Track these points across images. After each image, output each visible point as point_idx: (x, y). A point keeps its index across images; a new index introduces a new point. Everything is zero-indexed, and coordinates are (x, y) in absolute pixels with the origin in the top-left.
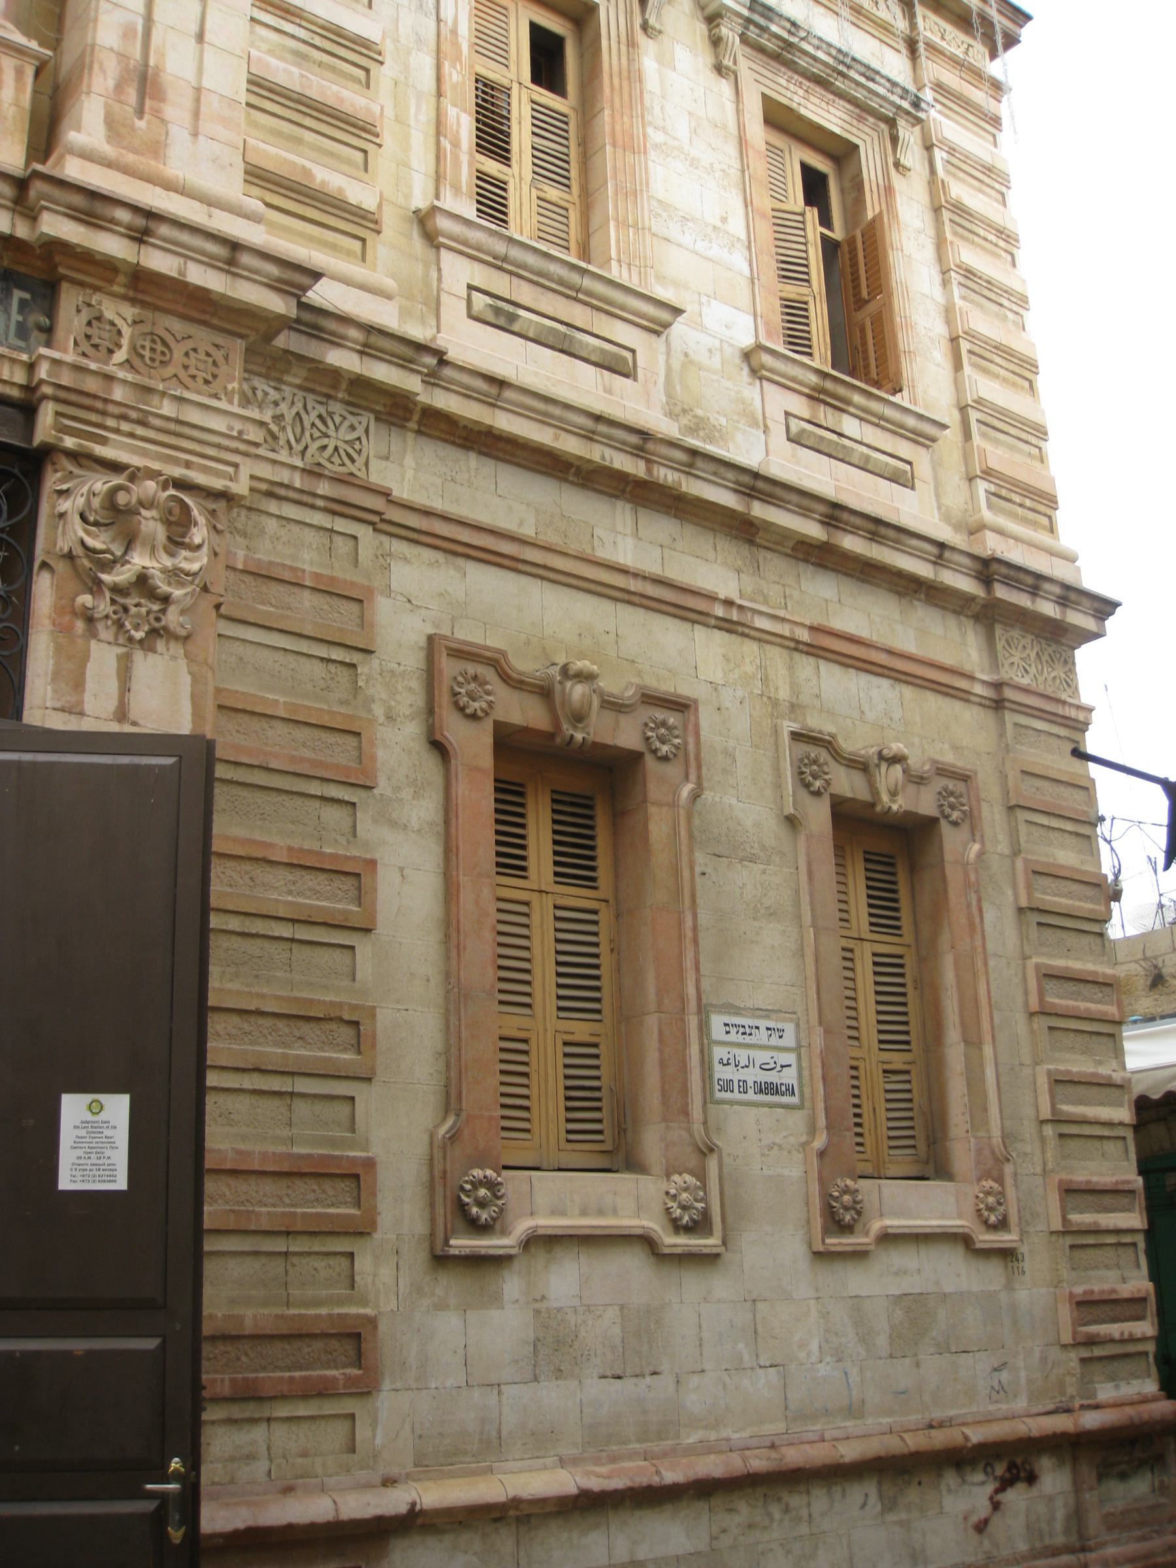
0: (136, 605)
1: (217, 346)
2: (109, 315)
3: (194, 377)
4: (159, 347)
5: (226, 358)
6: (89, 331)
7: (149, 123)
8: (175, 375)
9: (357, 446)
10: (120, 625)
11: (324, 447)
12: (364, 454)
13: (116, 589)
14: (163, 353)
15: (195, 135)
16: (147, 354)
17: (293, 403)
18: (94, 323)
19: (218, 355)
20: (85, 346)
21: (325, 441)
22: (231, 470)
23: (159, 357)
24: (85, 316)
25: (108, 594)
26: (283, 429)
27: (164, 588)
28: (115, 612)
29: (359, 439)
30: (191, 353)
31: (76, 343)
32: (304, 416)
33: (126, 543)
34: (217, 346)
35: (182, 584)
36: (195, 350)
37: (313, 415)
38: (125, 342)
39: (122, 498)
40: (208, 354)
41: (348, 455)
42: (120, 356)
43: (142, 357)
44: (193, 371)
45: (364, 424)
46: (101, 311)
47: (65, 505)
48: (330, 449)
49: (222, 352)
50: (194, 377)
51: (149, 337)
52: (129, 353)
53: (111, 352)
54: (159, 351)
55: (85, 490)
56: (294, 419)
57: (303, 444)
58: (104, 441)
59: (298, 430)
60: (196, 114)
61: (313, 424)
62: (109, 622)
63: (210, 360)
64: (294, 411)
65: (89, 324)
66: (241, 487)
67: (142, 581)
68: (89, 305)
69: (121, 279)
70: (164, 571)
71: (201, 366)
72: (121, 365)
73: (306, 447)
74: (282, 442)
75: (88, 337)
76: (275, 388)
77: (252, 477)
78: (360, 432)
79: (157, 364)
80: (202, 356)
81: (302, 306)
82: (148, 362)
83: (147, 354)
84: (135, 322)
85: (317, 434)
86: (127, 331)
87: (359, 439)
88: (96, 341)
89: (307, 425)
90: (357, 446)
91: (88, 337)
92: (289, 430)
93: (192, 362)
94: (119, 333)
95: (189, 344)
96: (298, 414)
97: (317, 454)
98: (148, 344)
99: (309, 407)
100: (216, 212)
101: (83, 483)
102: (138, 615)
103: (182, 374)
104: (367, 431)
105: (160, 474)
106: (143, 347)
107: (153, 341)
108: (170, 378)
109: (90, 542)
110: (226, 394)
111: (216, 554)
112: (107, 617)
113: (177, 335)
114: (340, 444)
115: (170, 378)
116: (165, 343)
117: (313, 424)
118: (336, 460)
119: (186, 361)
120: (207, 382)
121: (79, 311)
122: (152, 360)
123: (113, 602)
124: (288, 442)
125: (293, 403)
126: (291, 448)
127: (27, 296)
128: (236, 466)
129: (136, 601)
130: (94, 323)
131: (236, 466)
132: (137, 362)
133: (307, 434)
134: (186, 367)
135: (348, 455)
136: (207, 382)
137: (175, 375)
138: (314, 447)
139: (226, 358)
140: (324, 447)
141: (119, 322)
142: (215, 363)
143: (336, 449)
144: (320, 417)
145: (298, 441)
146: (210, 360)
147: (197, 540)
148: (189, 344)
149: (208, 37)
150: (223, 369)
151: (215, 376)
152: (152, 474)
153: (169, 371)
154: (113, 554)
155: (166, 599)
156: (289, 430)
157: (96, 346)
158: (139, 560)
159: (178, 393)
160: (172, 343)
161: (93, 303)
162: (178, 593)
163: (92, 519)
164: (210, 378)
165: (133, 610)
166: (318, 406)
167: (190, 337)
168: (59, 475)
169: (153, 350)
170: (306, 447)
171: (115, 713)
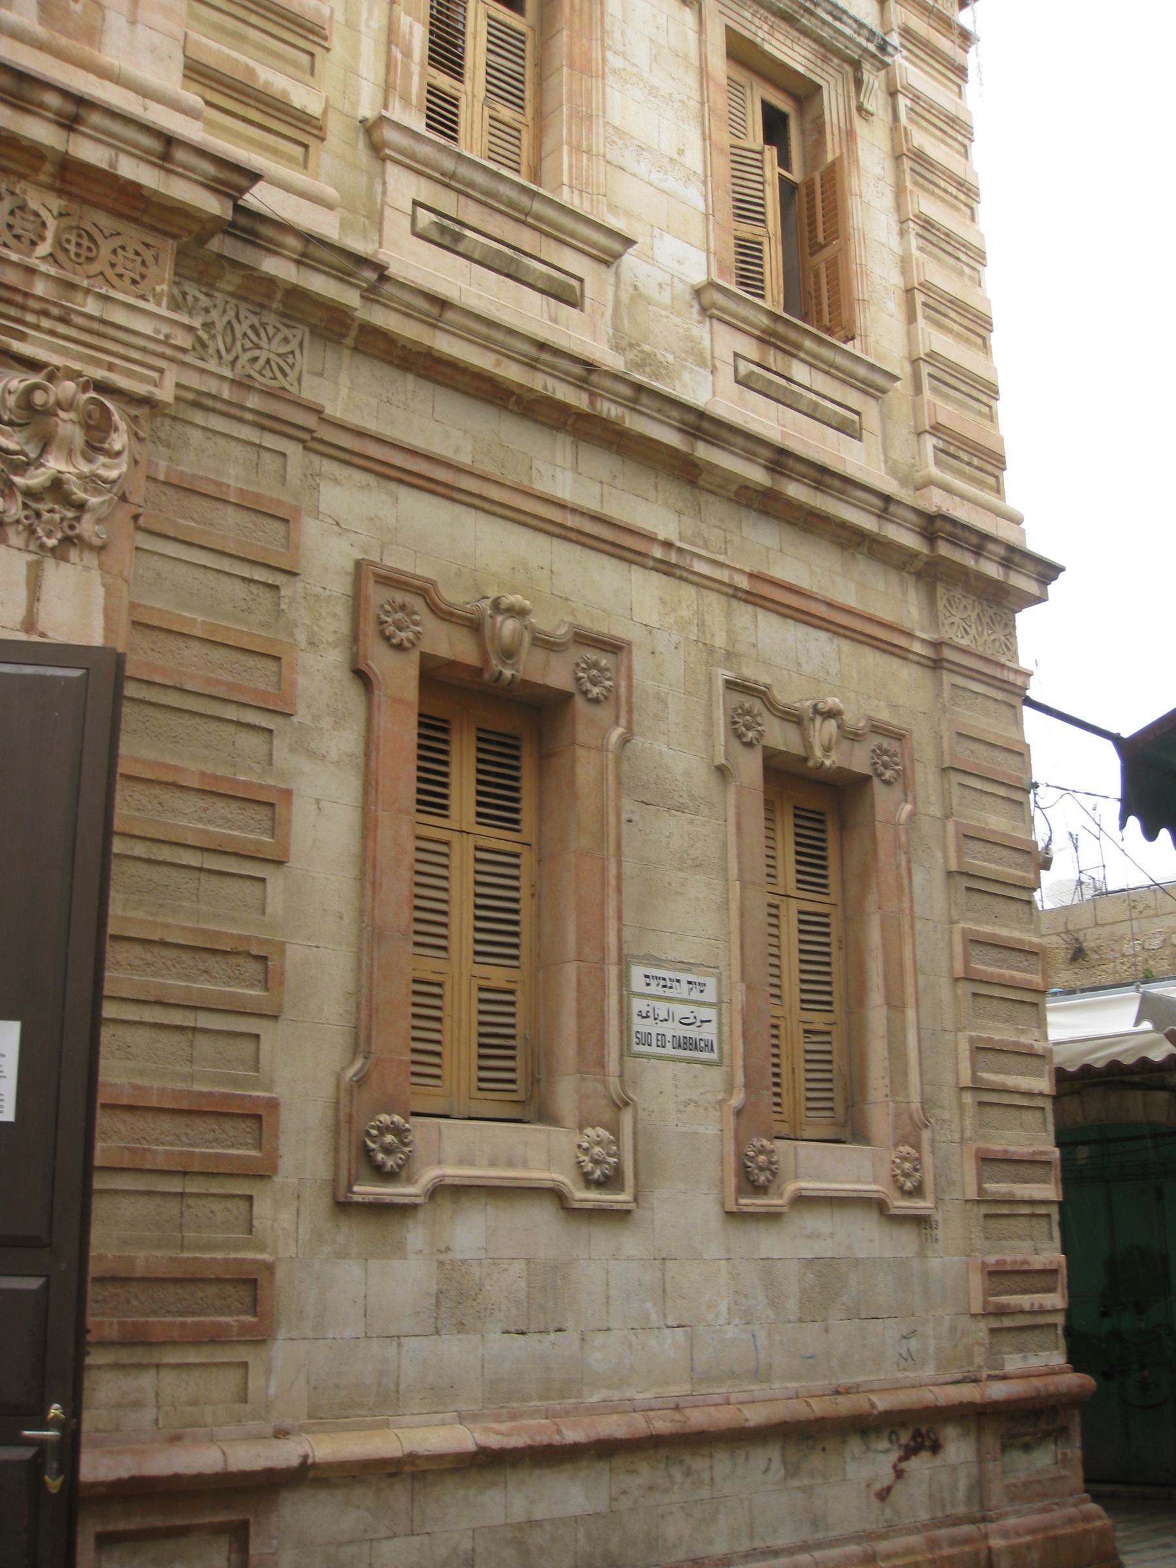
0: (51, 511)
1: (147, 245)
2: (33, 205)
3: (120, 276)
4: (85, 242)
5: (156, 258)
6: (12, 221)
8: (102, 273)
9: (290, 360)
10: (31, 531)
11: (255, 359)
12: (297, 368)
13: (30, 494)
14: (89, 249)
16: (72, 248)
17: (225, 311)
18: (18, 212)
19: (148, 255)
21: (257, 353)
22: (155, 375)
23: (84, 253)
25: (20, 498)
26: (214, 337)
27: (80, 494)
28: (27, 518)
29: (292, 352)
33: (41, 445)
34: (147, 245)
35: (98, 492)
36: (123, 248)
37: (245, 325)
38: (50, 234)
39: (39, 398)
40: (137, 253)
42: (44, 249)
43: (67, 251)
45: (299, 338)
46: (25, 201)
48: (262, 362)
49: (152, 252)
50: (120, 276)
51: (75, 231)
52: (53, 246)
53: (33, 243)
54: (85, 246)
56: (225, 328)
57: (234, 354)
58: (22, 337)
59: (229, 339)
62: (20, 528)
64: (225, 319)
65: (12, 213)
66: (165, 394)
67: (57, 485)
68: (13, 193)
69: (48, 167)
70: (81, 476)
71: (130, 265)
72: (43, 258)
73: (237, 358)
74: (211, 351)
76: (207, 295)
77: (178, 385)
78: (293, 345)
79: (82, 260)
80: (130, 255)
81: (239, 209)
82: (73, 257)
83: (72, 248)
84: (61, 215)
85: (248, 345)
86: (52, 224)
87: (292, 352)
88: (19, 231)
89: (239, 334)
90: (290, 360)
92: (220, 338)
93: (119, 260)
94: (44, 225)
95: (117, 242)
96: (229, 323)
97: (248, 366)
98: (73, 238)
99: (242, 317)
100: (152, 105)
102: (51, 522)
103: (110, 273)
104: (301, 345)
105: (80, 374)
106: (68, 241)
107: (80, 236)
108: (95, 276)
110: (154, 296)
111: (136, 462)
112: (18, 522)
113: (104, 230)
114: (273, 357)
115: (95, 276)
116: (92, 239)
117: (245, 335)
118: (267, 373)
119: (113, 259)
120: (134, 282)
122: (78, 255)
123: (25, 506)
124: (218, 351)
125: (225, 311)
126: (220, 357)
128: (161, 371)
129: (50, 506)
130: (18, 212)
131: (161, 371)
132: (61, 257)
133: (238, 344)
134: (113, 265)
136: (134, 282)
137: (102, 273)
139: (156, 258)
140: (255, 359)
142: (144, 263)
143: (268, 361)
144: (252, 327)
145: (228, 351)
146: (139, 259)
147: (117, 447)
150: (152, 269)
151: (143, 277)
152: (73, 375)
153: (95, 268)
154: (26, 455)
155: (81, 507)
156: (220, 338)
158: (55, 464)
159: (103, 291)
160: (100, 239)
161: (18, 191)
162: (93, 500)
164: (138, 278)
165: (46, 516)
166: (251, 316)
167: (118, 234)
169: (79, 245)
170: (237, 358)
171: (22, 623)
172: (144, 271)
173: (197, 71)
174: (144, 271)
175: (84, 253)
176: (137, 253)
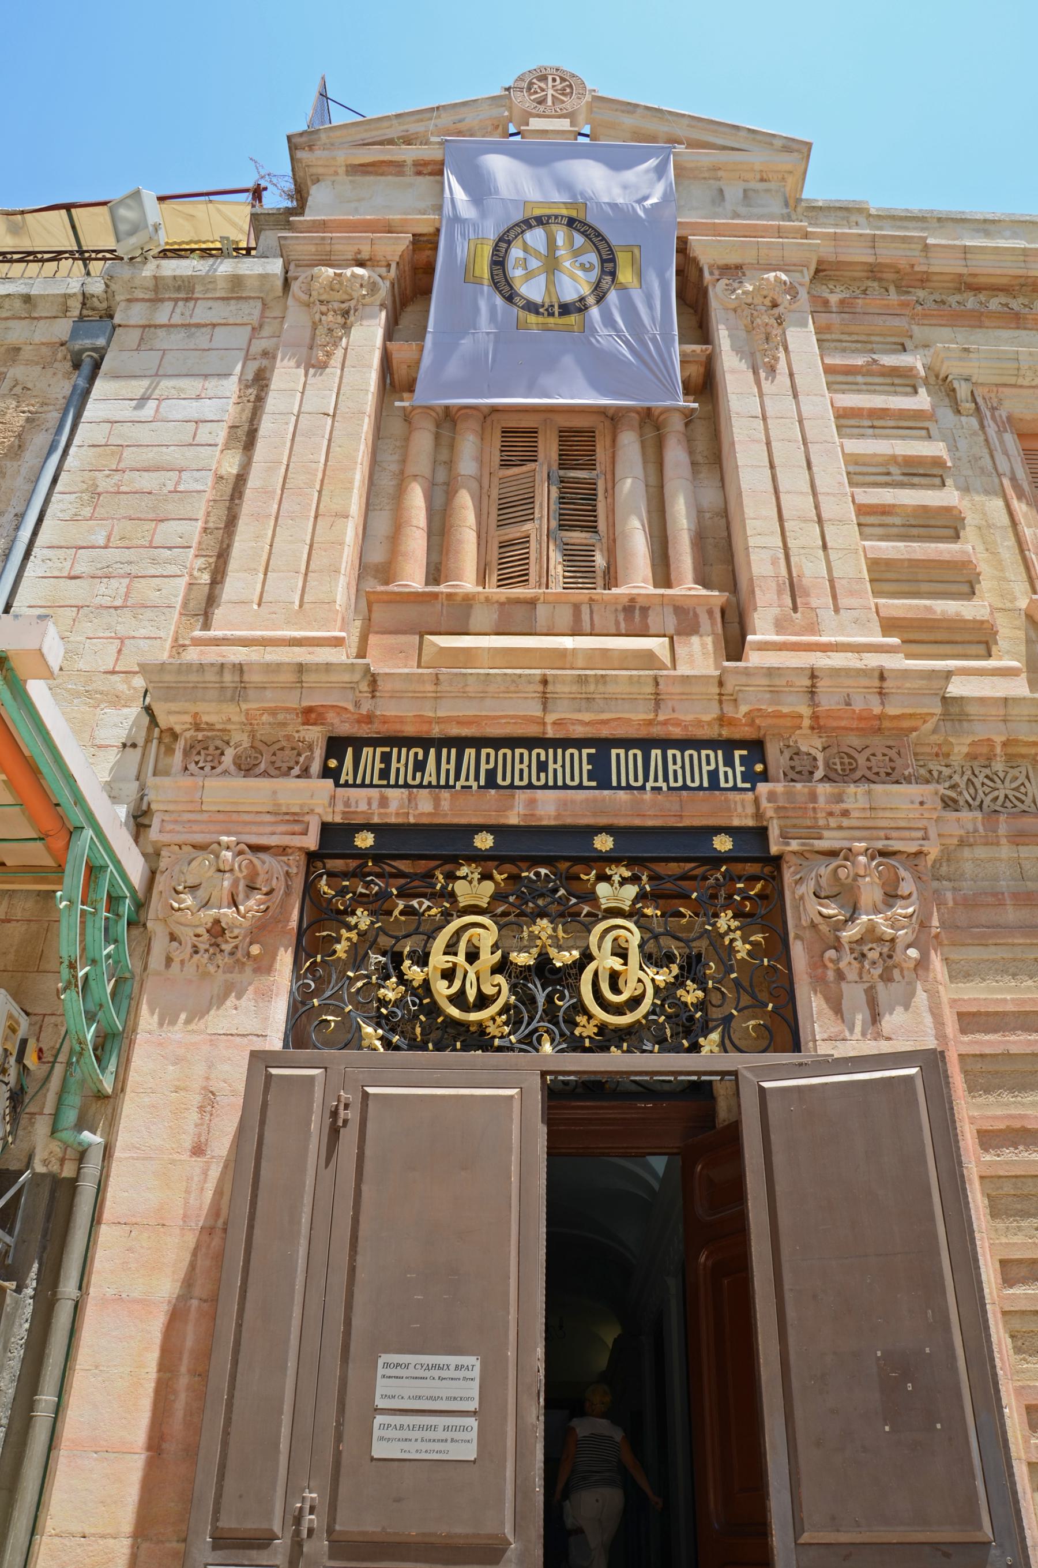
1: (890, 747)
2: (804, 749)
3: (877, 774)
4: (846, 760)
5: (899, 754)
6: (793, 763)
7: (803, 613)
8: (863, 776)
9: (1023, 790)
11: (997, 798)
12: (1030, 794)
15: (837, 610)
17: (963, 773)
18: (795, 757)
20: (792, 775)
21: (996, 793)
24: (787, 754)
26: (961, 793)
29: (1023, 784)
30: (872, 758)
31: (785, 774)
32: (975, 780)
34: (890, 747)
36: (874, 755)
37: (981, 777)
38: (820, 763)
40: (884, 755)
41: (1017, 798)
43: (836, 770)
44: (875, 770)
45: (1024, 773)
46: (798, 748)
47: (802, 890)
48: (1001, 798)
49: (895, 750)
52: (825, 770)
53: (811, 773)
55: (813, 875)
56: (967, 784)
57: (979, 800)
59: (972, 791)
60: (834, 597)
61: (983, 784)
63: (887, 758)
64: (965, 778)
65: (791, 759)
68: (788, 746)
71: (881, 765)
72: (821, 780)
73: (982, 802)
74: (962, 803)
75: (793, 768)
76: (947, 766)
78: (1022, 779)
79: (848, 772)
80: (880, 757)
84: (824, 749)
85: (988, 790)
86: (820, 756)
87: (1023, 784)
89: (978, 785)
90: (1023, 790)
91: (793, 768)
92: (965, 793)
94: (815, 759)
95: (867, 752)
96: (969, 780)
97: (992, 804)
99: (976, 772)
100: (865, 655)
101: (811, 871)
104: (1028, 777)
106: (835, 764)
109: (825, 911)
110: (905, 779)
114: (1008, 792)
117: (983, 784)
118: (1008, 804)
121: (782, 752)
122: (843, 770)
124: (967, 802)
125: (963, 773)
126: (970, 805)
127: (745, 752)
130: (795, 757)
132: (832, 775)
133: (980, 792)
134: (870, 768)
135: (1017, 798)
136: (888, 774)
137: (863, 776)
138: (987, 800)
139: (899, 754)
140: (997, 798)
141: (813, 751)
142: (891, 760)
143: (1006, 796)
144: (987, 777)
145: (974, 799)
146: (887, 758)
147: (907, 893)
148: (867, 752)
149: (829, 544)
151: (893, 769)
156: (965, 793)
157: (800, 773)
163: (823, 895)
164: (890, 771)
166: (983, 769)
167: (867, 747)
168: (792, 869)
170: (982, 802)
172: (892, 764)
173: (889, 626)
174: (892, 764)
175: (847, 767)
176: (884, 755)
